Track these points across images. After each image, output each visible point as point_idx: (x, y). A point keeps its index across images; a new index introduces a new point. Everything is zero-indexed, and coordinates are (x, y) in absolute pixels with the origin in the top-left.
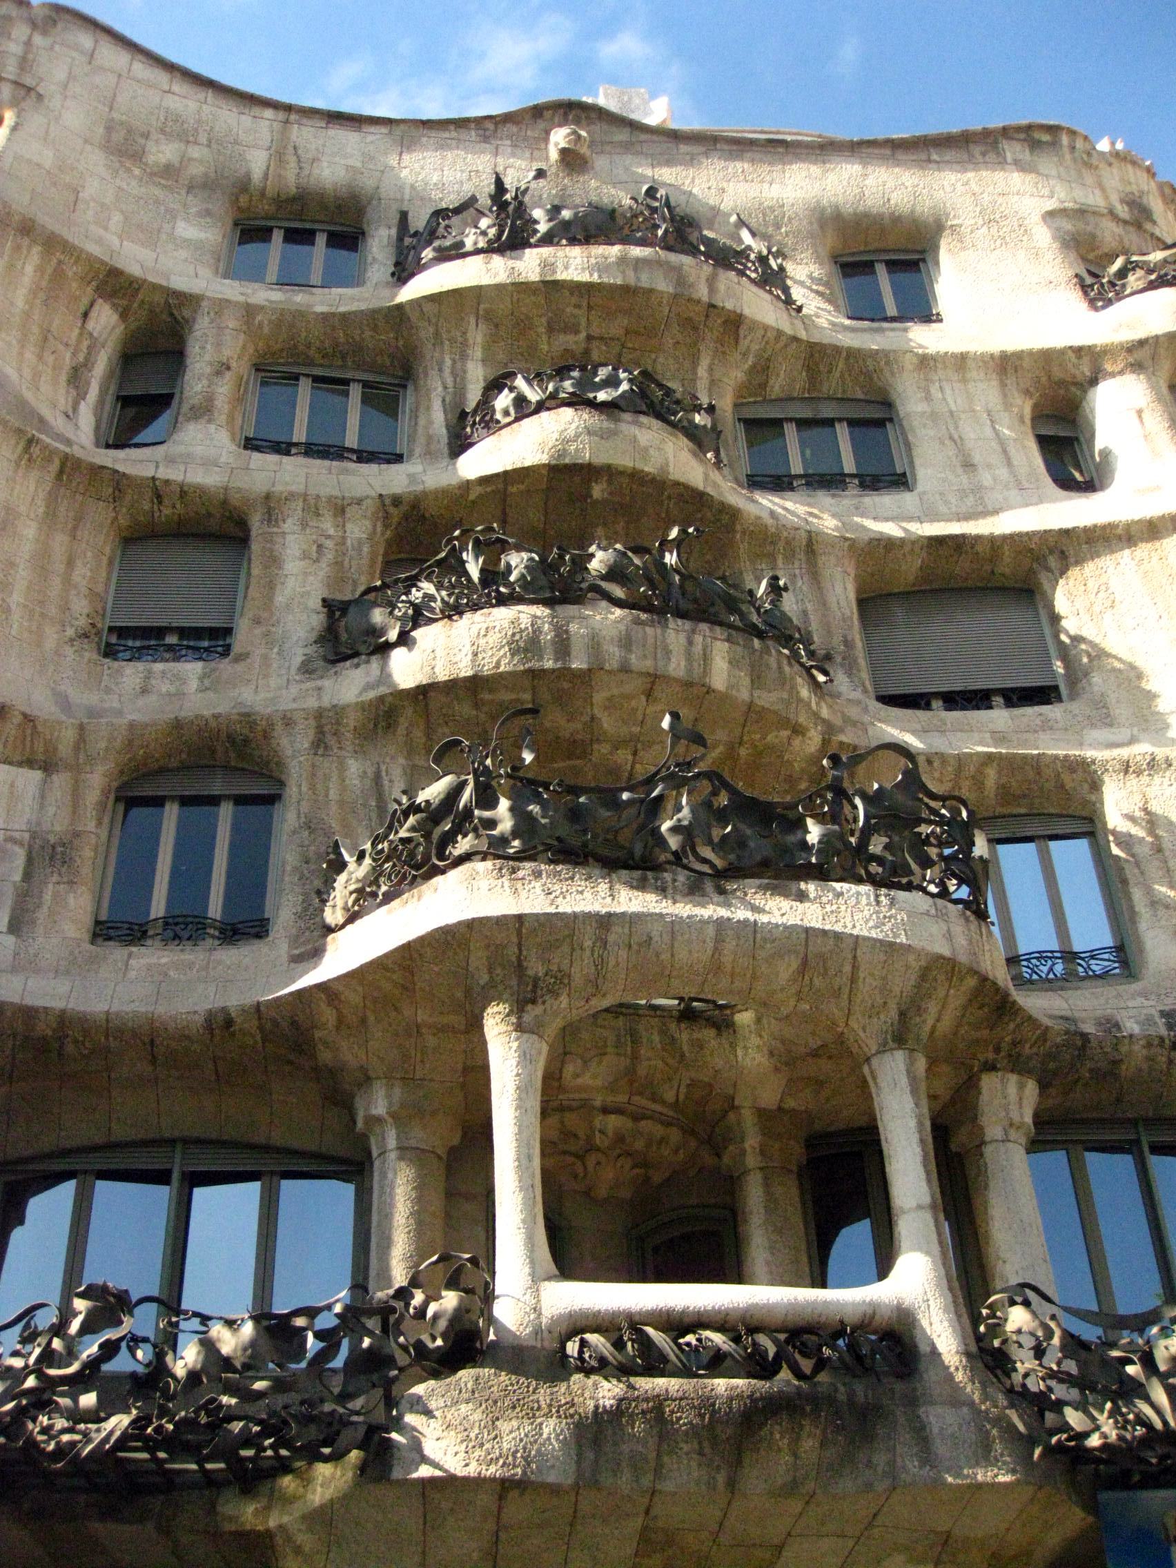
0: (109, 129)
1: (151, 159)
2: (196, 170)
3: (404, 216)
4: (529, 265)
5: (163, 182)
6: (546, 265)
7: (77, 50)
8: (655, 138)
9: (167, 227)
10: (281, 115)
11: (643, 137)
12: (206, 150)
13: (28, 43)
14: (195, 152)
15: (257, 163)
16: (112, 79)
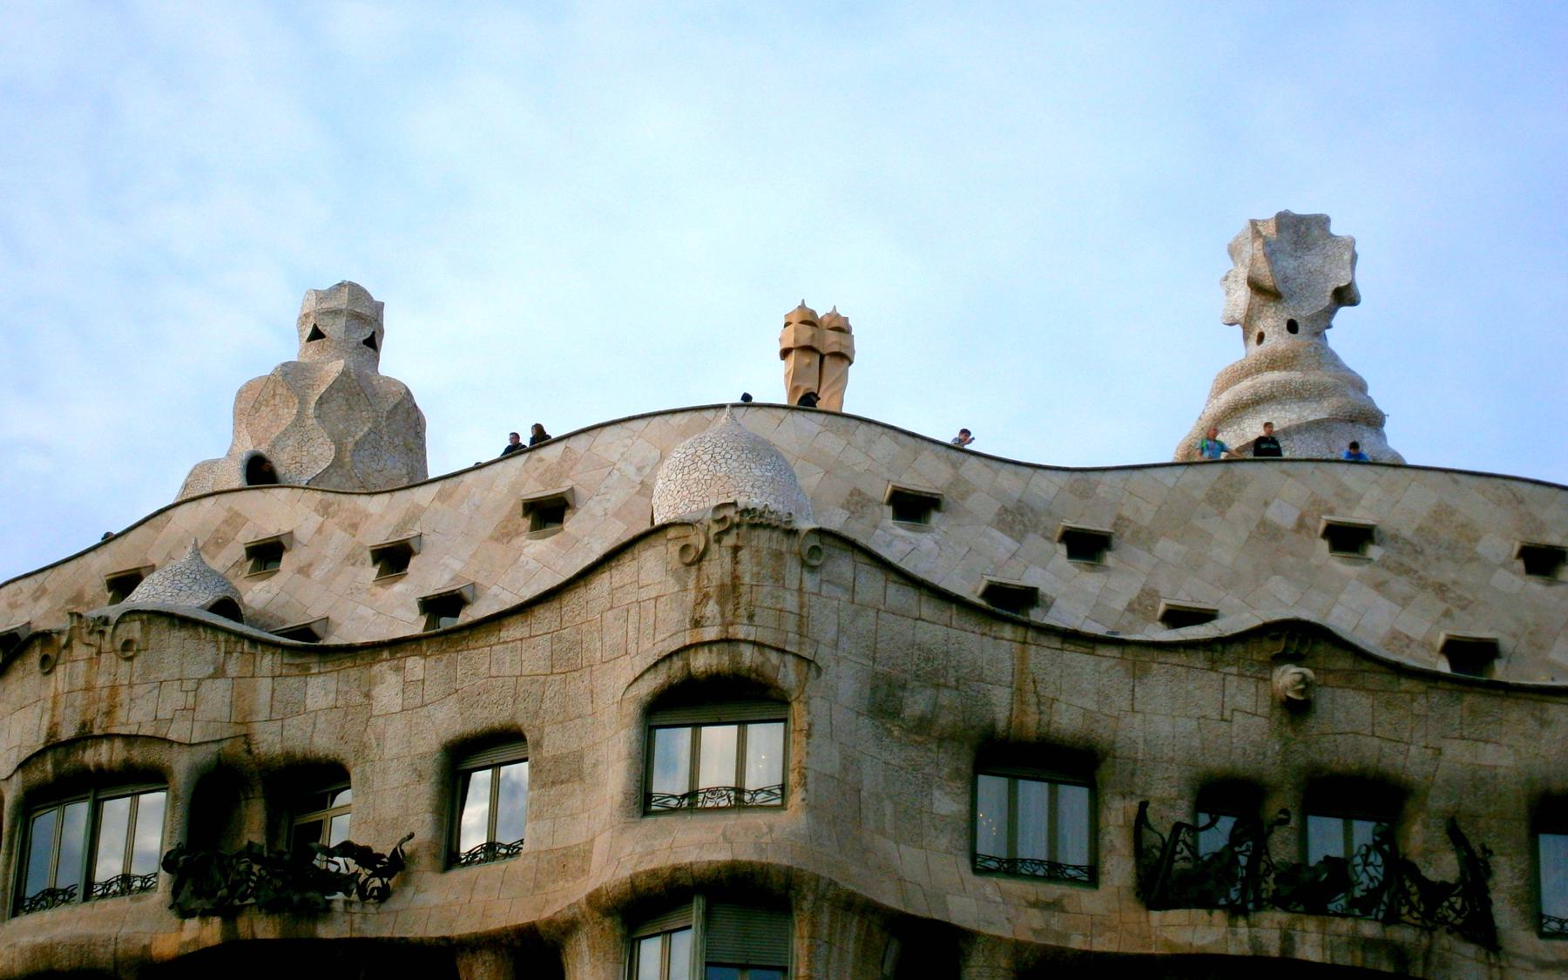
0: (875, 689)
1: (907, 713)
2: (945, 720)
3: (1144, 806)
4: (1268, 931)
5: (918, 739)
6: (1287, 939)
7: (838, 585)
8: (1377, 667)
9: (926, 801)
10: (1020, 631)
11: (1366, 665)
12: (955, 693)
13: (800, 590)
14: (946, 698)
15: (1000, 707)
16: (872, 613)
